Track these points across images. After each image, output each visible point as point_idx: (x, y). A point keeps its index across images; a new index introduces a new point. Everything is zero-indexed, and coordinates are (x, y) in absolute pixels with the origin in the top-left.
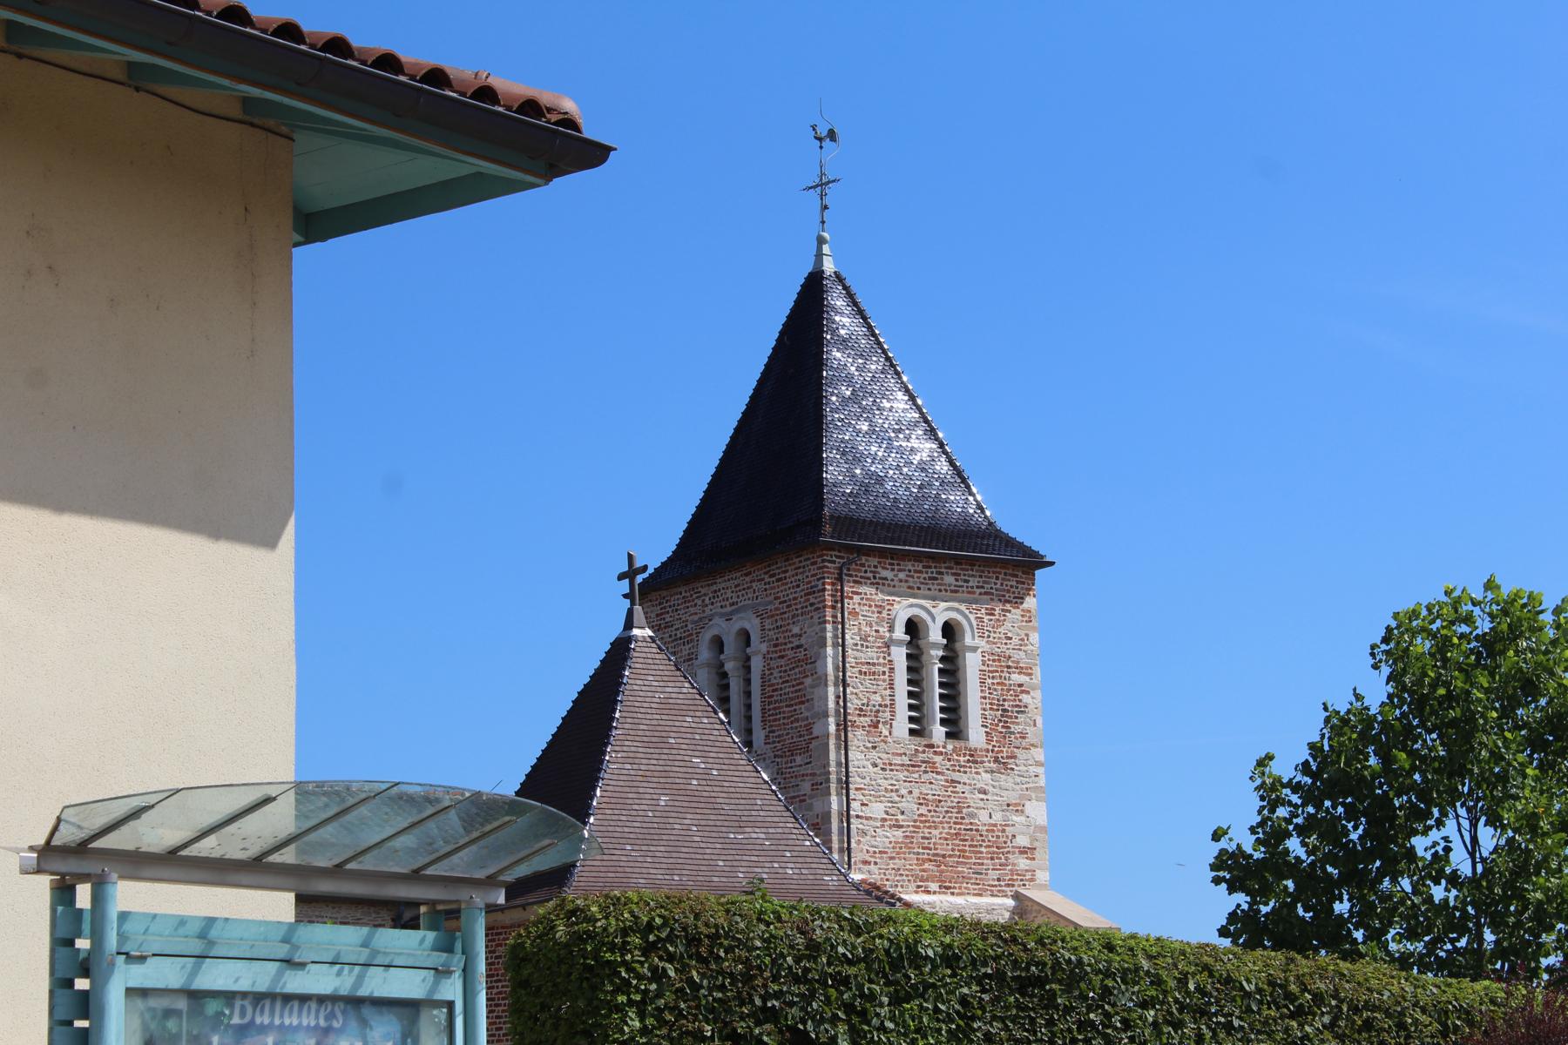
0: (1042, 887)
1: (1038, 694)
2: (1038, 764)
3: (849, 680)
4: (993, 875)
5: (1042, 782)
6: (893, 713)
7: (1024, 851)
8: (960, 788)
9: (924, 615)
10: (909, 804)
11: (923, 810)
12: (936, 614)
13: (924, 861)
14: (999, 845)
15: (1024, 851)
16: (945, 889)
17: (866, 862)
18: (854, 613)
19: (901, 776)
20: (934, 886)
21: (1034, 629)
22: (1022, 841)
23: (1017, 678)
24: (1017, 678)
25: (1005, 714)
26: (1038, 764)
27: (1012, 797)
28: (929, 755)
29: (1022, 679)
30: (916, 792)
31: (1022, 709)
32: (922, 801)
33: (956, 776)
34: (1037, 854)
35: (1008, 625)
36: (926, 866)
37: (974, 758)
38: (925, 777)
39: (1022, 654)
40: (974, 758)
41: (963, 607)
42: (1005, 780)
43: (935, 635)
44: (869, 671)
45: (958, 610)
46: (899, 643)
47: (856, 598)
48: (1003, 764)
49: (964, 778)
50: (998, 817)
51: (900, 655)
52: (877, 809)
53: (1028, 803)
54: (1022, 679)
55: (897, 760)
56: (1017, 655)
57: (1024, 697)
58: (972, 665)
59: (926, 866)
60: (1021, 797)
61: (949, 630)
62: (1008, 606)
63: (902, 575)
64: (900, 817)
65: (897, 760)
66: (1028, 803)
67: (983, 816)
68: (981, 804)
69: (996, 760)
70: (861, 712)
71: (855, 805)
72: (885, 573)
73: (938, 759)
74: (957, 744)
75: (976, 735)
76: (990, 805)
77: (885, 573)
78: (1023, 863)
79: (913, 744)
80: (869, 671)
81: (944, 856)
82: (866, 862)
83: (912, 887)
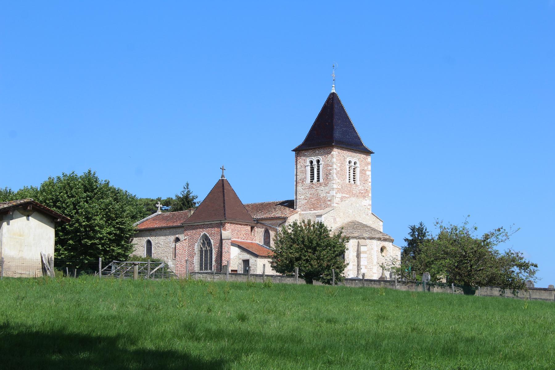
7: (329, 201)
10: (308, 195)
12: (314, 159)
15: (329, 201)
22: (329, 199)
23: (329, 168)
24: (329, 168)
25: (328, 175)
27: (327, 191)
46: (308, 166)
50: (325, 195)
51: (309, 169)
52: (303, 197)
67: (322, 195)
75: (321, 180)
78: (329, 203)
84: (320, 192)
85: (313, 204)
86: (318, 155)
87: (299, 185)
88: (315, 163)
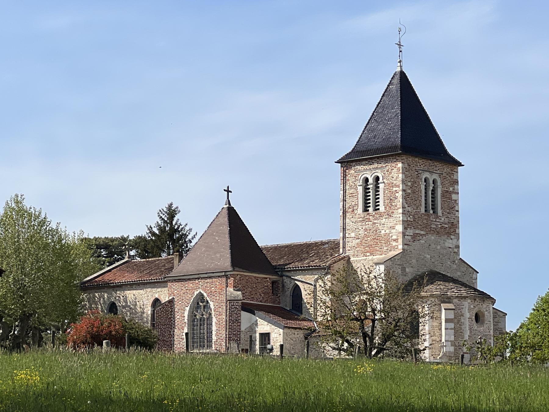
4: (386, 248)
7: (395, 240)
8: (376, 224)
11: (366, 233)
15: (395, 240)
19: (360, 224)
20: (368, 254)
22: (394, 237)
23: (394, 189)
24: (394, 189)
25: (391, 200)
30: (364, 228)
31: (396, 198)
32: (366, 230)
33: (375, 221)
37: (381, 215)
38: (367, 223)
50: (387, 231)
52: (353, 235)
55: (359, 220)
56: (395, 182)
57: (397, 194)
65: (359, 220)
67: (383, 232)
69: (388, 214)
71: (346, 235)
75: (382, 208)
78: (394, 244)
85: (370, 246)
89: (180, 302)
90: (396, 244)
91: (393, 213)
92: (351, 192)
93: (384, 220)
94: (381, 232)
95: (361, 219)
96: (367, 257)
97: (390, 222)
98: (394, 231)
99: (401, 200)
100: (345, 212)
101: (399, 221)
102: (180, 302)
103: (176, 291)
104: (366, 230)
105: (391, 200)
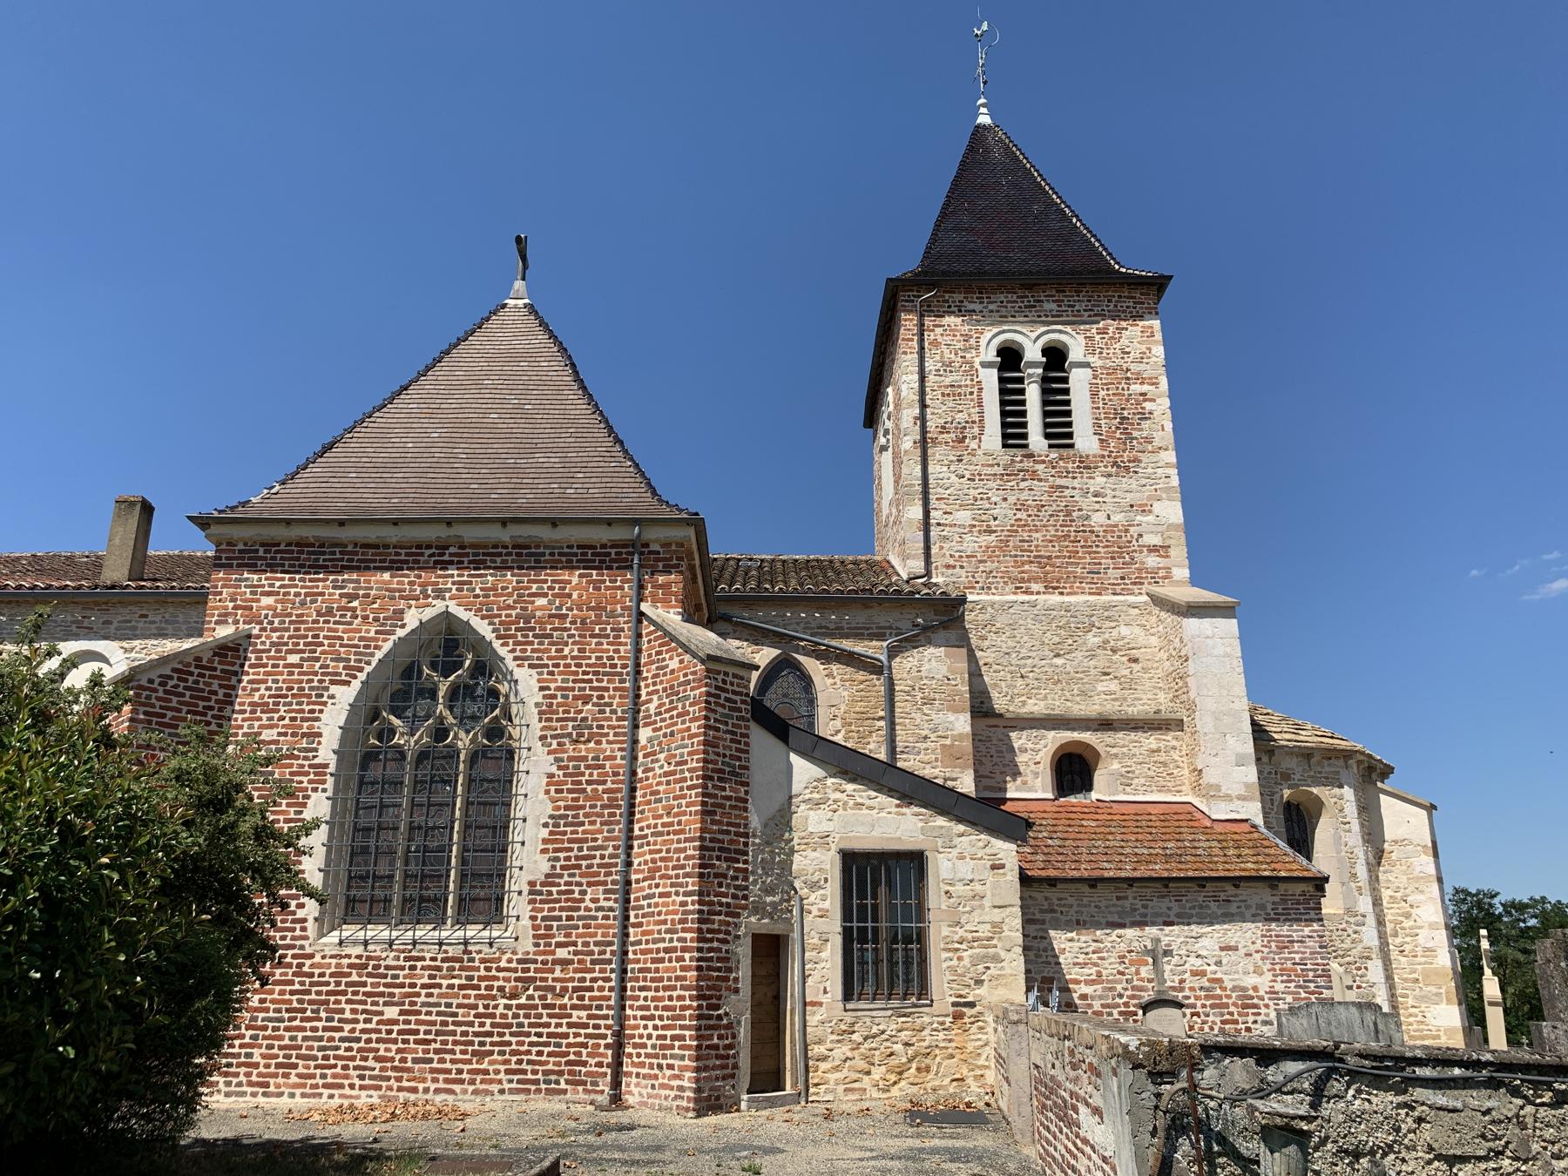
0: (1179, 583)
1: (1166, 402)
2: (1168, 465)
3: (928, 402)
5: (1175, 481)
6: (982, 428)
7: (1153, 549)
8: (1067, 492)
9: (1018, 338)
11: (1022, 515)
13: (1023, 564)
14: (1122, 546)
16: (1050, 588)
17: (948, 567)
18: (935, 343)
19: (991, 484)
20: (1035, 587)
21: (1156, 342)
22: (1151, 539)
23: (1136, 388)
24: (1136, 388)
25: (1123, 424)
26: (1168, 465)
28: (1027, 464)
29: (1145, 388)
30: (1012, 499)
31: (1145, 416)
33: (1059, 482)
34: (1172, 552)
35: (1124, 341)
36: (1027, 567)
37: (1086, 464)
38: (1023, 485)
39: (1142, 367)
40: (1086, 464)
41: (1068, 329)
42: (1126, 482)
43: (1033, 353)
44: (953, 392)
45: (1060, 332)
47: (939, 330)
48: (1122, 468)
49: (1076, 483)
50: (1116, 518)
51: (990, 378)
53: (1156, 504)
54: (1145, 388)
55: (990, 471)
57: (1148, 406)
58: (1079, 381)
59: (1027, 567)
60: (1149, 498)
61: (1055, 357)
62: (1124, 324)
63: (991, 307)
64: (992, 523)
65: (990, 471)
66: (1156, 504)
67: (1098, 519)
68: (1097, 506)
69: (1115, 464)
70: (944, 429)
72: (971, 307)
73: (1038, 467)
74: (1065, 452)
75: (1085, 439)
76: (1109, 508)
77: (971, 307)
78: (1152, 561)
79: (1004, 456)
80: (953, 392)
81: (1049, 558)
82: (948, 567)
83: (1011, 587)
84: (1087, 503)
85: (1043, 561)
86: (1057, 318)
87: (936, 453)
88: (1033, 353)
89: (294, 659)
90: (1163, 562)
91: (1136, 460)
92: (948, 381)
93: (1101, 480)
94: (1088, 517)
95: (999, 470)
96: (1034, 597)
97: (1130, 488)
98: (1150, 518)
99: (1169, 426)
100: (924, 443)
101: (1169, 489)
102: (294, 659)
103: (267, 601)
104: (1021, 506)
105: (1123, 424)
